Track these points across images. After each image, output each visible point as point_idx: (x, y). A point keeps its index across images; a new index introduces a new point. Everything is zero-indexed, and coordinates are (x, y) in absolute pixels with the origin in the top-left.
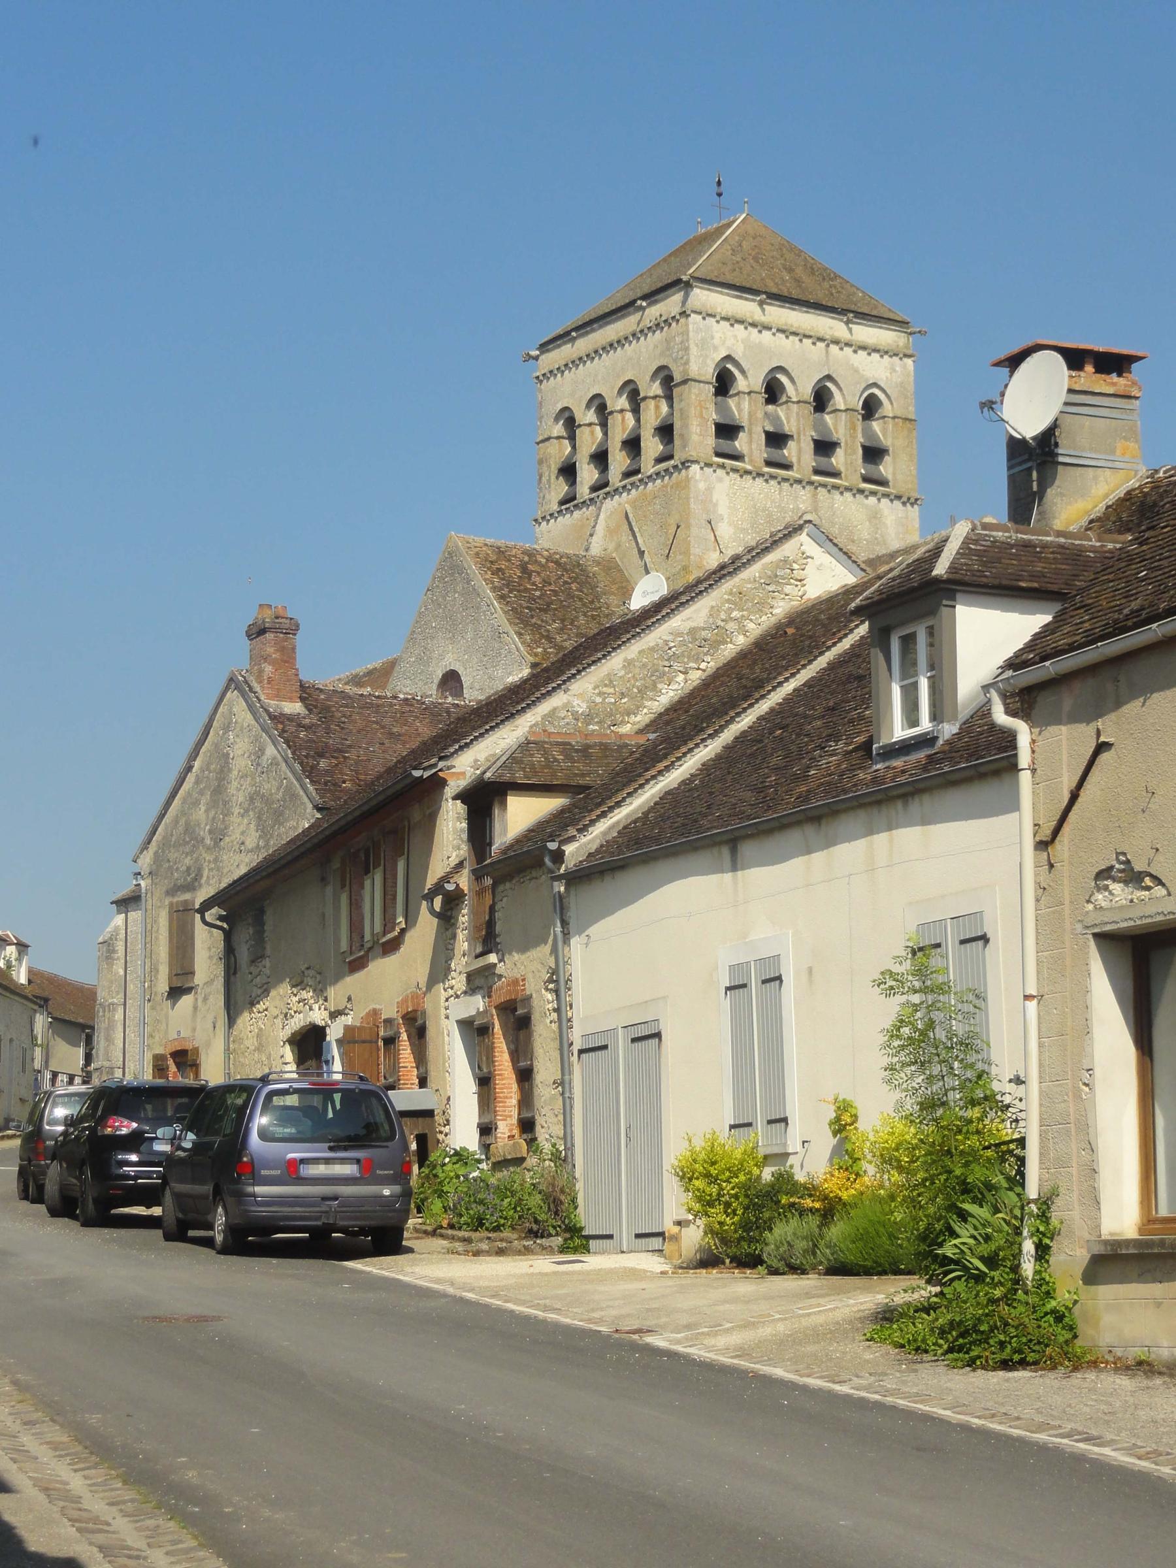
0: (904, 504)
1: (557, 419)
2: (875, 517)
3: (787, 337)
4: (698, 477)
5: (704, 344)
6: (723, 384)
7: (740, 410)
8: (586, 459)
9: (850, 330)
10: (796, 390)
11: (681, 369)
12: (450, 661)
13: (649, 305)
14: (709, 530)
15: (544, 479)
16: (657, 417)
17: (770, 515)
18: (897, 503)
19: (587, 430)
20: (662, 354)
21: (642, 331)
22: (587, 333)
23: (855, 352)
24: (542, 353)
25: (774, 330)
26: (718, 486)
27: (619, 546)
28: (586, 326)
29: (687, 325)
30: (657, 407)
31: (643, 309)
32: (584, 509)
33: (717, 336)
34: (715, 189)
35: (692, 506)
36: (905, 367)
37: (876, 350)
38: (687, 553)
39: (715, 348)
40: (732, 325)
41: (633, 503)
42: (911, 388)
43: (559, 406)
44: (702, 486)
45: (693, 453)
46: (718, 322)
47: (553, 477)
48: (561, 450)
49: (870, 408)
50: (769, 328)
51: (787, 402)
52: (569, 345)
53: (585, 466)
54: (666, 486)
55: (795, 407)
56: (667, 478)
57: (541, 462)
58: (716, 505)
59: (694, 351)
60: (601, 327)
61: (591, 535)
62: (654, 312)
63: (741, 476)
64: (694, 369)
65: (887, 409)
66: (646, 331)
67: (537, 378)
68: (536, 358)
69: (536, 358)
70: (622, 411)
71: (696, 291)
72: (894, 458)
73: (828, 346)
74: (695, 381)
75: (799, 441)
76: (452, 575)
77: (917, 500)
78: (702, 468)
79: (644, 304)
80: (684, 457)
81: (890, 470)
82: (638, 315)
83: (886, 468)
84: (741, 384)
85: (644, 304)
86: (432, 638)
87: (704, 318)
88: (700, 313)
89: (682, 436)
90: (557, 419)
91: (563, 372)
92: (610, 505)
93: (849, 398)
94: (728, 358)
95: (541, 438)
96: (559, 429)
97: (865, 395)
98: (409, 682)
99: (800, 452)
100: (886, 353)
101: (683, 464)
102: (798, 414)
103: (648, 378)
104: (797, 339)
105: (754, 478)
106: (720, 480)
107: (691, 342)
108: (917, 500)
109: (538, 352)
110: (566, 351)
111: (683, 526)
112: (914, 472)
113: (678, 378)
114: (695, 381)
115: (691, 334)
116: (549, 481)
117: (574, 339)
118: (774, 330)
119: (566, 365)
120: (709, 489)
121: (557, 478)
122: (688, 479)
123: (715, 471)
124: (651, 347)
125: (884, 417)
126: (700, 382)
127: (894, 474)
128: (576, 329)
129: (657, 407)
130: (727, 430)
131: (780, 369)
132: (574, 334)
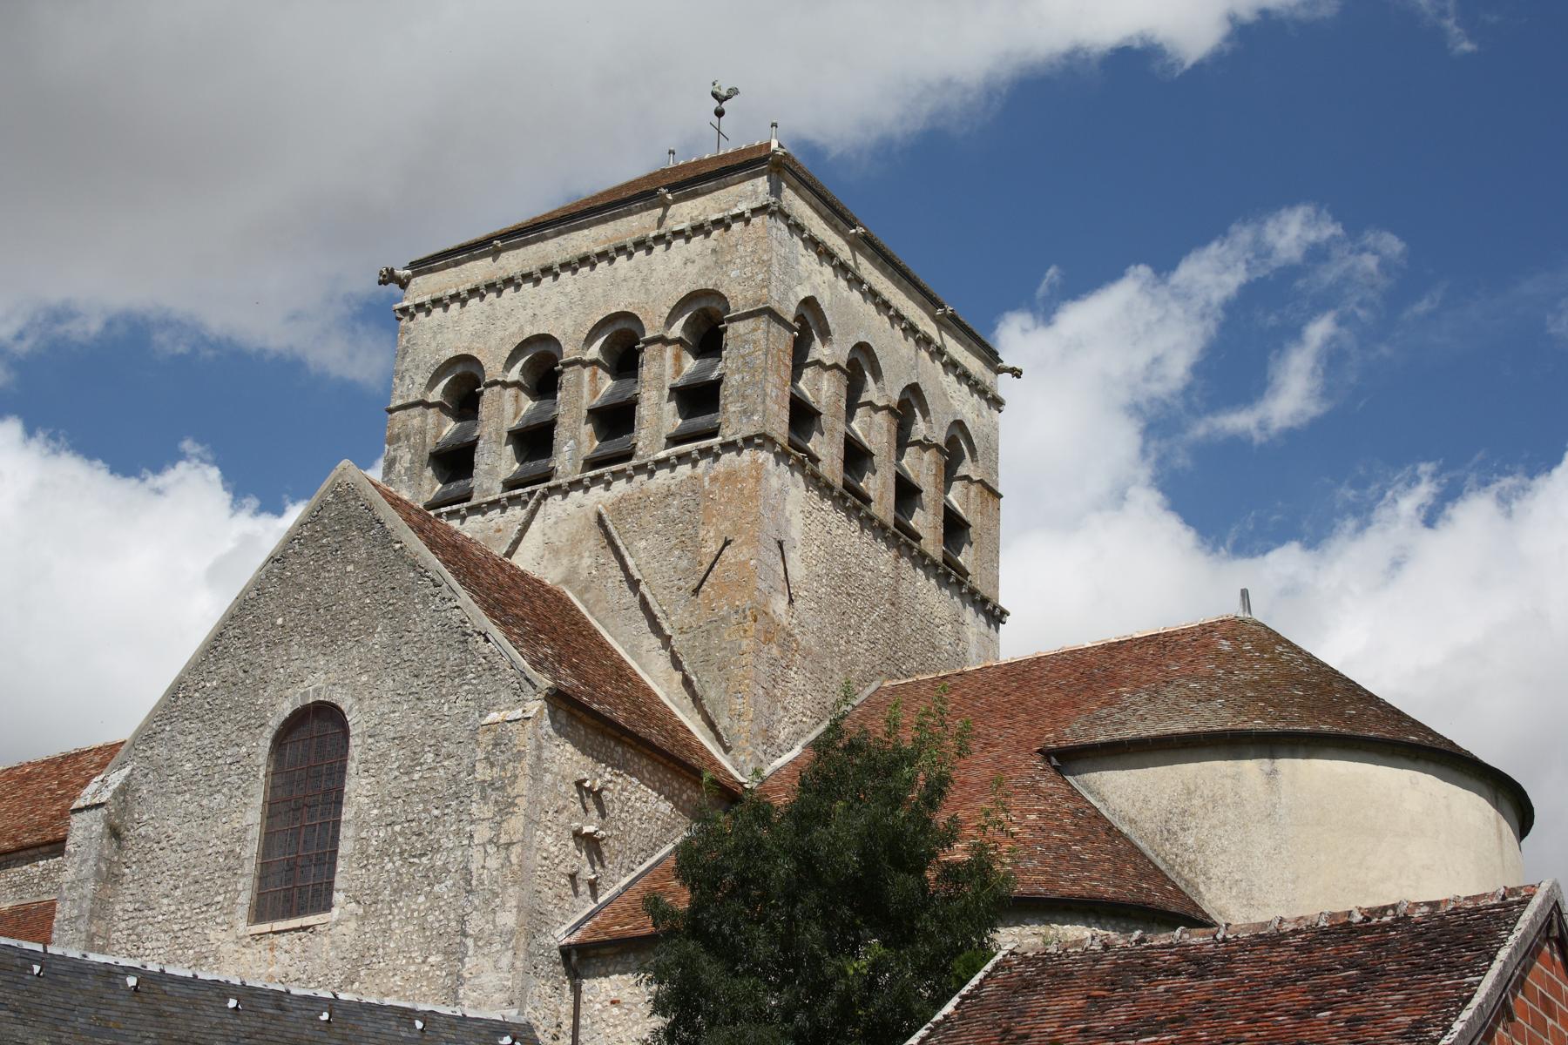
2: (957, 621)
12: (316, 686)
13: (676, 201)
17: (846, 566)
24: (416, 274)
26: (793, 491)
30: (677, 358)
31: (666, 206)
44: (775, 483)
56: (702, 464)
62: (685, 213)
67: (404, 310)
68: (403, 284)
76: (342, 532)
85: (669, 197)
94: (810, 303)
95: (399, 402)
109: (408, 272)
110: (479, 270)
113: (738, 304)
120: (783, 491)
130: (803, 415)
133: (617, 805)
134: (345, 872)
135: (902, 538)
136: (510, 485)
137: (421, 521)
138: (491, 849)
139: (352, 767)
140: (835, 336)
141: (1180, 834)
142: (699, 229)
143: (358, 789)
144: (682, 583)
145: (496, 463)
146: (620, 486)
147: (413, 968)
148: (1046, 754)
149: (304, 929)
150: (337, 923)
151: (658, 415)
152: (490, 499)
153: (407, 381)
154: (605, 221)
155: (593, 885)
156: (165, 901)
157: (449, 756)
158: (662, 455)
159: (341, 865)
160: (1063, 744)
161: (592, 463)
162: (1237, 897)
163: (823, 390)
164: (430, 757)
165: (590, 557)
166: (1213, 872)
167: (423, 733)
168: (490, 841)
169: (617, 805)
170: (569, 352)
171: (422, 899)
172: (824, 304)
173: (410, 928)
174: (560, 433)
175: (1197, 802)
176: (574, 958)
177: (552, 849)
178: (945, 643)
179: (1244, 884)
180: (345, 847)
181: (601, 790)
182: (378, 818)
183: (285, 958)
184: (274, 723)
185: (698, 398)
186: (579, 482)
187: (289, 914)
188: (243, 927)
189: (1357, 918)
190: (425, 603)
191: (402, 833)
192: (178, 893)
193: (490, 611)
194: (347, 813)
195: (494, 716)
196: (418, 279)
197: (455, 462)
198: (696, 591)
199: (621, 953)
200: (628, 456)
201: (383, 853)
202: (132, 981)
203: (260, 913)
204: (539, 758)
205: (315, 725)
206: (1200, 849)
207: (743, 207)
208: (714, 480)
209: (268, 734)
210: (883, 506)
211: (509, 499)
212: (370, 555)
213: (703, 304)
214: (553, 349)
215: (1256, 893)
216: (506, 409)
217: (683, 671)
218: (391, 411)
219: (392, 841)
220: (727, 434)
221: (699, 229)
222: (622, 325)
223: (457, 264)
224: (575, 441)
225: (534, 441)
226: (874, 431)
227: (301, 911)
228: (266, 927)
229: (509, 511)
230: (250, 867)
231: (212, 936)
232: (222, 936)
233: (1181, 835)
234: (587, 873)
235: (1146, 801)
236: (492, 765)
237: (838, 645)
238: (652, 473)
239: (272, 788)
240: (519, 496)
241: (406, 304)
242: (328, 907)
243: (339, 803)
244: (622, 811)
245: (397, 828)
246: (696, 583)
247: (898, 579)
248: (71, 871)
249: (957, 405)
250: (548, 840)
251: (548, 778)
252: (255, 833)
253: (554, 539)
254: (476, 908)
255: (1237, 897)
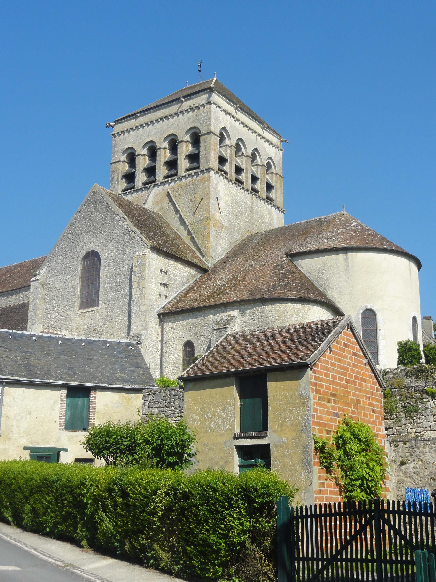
0: (279, 211)
1: (123, 153)
2: (270, 214)
3: (244, 127)
4: (213, 177)
5: (216, 118)
6: (222, 138)
7: (226, 153)
8: (141, 170)
9: (263, 132)
10: (246, 151)
11: (206, 128)
12: (92, 246)
13: (186, 101)
14: (217, 202)
15: (114, 180)
16: (187, 151)
17: (237, 202)
18: (277, 210)
19: (142, 157)
20: (193, 122)
21: (181, 112)
22: (146, 114)
23: (265, 141)
24: (116, 124)
25: (240, 122)
26: (220, 183)
27: (161, 209)
28: (143, 112)
29: (210, 108)
30: (187, 146)
31: (182, 102)
32: (140, 192)
33: (221, 117)
34: (198, 68)
35: (211, 189)
36: (279, 154)
37: (272, 144)
38: (208, 210)
39: (220, 122)
40: (226, 114)
41: (173, 189)
42: (281, 163)
43: (126, 147)
44: (215, 181)
45: (212, 166)
46: (221, 111)
47: (120, 179)
48: (124, 167)
49: (269, 166)
50: (238, 120)
51: (242, 155)
52: (134, 120)
53: (140, 173)
54: (195, 180)
55: (245, 158)
56: (195, 177)
57: (113, 172)
58: (219, 192)
59: (213, 120)
60: (154, 111)
61: (145, 204)
62: (187, 104)
63: (228, 181)
64: (213, 129)
65: (273, 170)
66: (184, 112)
67: (113, 135)
68: (113, 127)
69: (113, 127)
70: (165, 148)
71: (214, 95)
72: (275, 190)
73: (257, 136)
74: (214, 133)
75: (246, 173)
77: (284, 210)
78: (215, 173)
79: (183, 100)
80: (207, 167)
81: (274, 196)
82: (178, 106)
83: (272, 195)
84: (227, 142)
85: (183, 100)
86: (79, 235)
87: (217, 107)
88: (215, 104)
89: (205, 158)
90: (123, 153)
91: (129, 132)
92: (156, 190)
93: (263, 160)
94: (224, 128)
95: (114, 161)
96: (124, 158)
97: (267, 161)
98: (61, 257)
99: (245, 177)
100: (275, 146)
101: (207, 170)
102: (246, 161)
103: (184, 133)
104: (247, 129)
105: (232, 184)
106: (221, 181)
107: (212, 116)
108: (284, 210)
109: (114, 124)
110: (132, 123)
111: (205, 198)
112: (282, 199)
113: (203, 131)
114: (214, 133)
115: (212, 113)
116: (118, 180)
117: (138, 117)
118: (240, 122)
119: (132, 129)
120: (217, 184)
121: (122, 180)
122: (209, 177)
123: (219, 176)
124: (186, 119)
125: (273, 173)
126: (215, 134)
127: (276, 198)
128: (139, 113)
129: (187, 146)
130: (222, 160)
131: (240, 139)
132: (138, 115)
133: (172, 275)
134: (102, 296)
135: (254, 191)
136: (145, 184)
137: (117, 200)
138: (138, 289)
139: (102, 268)
140: (231, 138)
141: (322, 276)
142: (192, 109)
143: (104, 274)
144: (191, 211)
145: (141, 178)
146: (173, 184)
147: (120, 321)
148: (287, 255)
149: (92, 311)
150: (100, 309)
151: (183, 164)
152: (139, 188)
153: (116, 155)
154: (166, 107)
155: (166, 297)
156: (57, 304)
157: (126, 264)
158: (184, 174)
159: (100, 294)
160: (291, 252)
161: (166, 177)
162: (337, 292)
163: (228, 153)
164: (121, 265)
165: (167, 204)
166: (331, 286)
167: (119, 258)
168: (137, 287)
169: (172, 275)
170: (158, 146)
171: (121, 303)
172: (228, 129)
173: (119, 310)
174: (157, 169)
175: (326, 267)
176: (161, 317)
177: (154, 288)
178: (267, 221)
179: (339, 289)
180: (101, 289)
181: (167, 271)
182: (109, 281)
183: (88, 319)
184: (81, 256)
185: (194, 158)
186: (163, 183)
187: (88, 307)
188: (77, 311)
189: (306, 324)
190: (118, 223)
191: (115, 285)
192: (59, 302)
193: (136, 225)
194: (101, 280)
195: (137, 254)
196: (117, 126)
197: (130, 177)
198: (194, 213)
199: (173, 315)
200: (176, 175)
201: (111, 291)
202: (34, 338)
203: (82, 307)
204: (149, 264)
205: (92, 258)
206: (327, 280)
207: (204, 102)
208: (198, 181)
209: (80, 259)
210: (248, 184)
211: (144, 188)
212: (103, 210)
213: (194, 131)
214: (154, 145)
215: (342, 291)
216: (143, 162)
217: (192, 235)
218: (111, 164)
219: (112, 287)
220: (202, 168)
221: (192, 109)
222: (172, 137)
223: (127, 121)
224: (162, 171)
225: (151, 171)
226: (244, 163)
227: (91, 306)
228: (82, 311)
229: (144, 192)
230: (78, 295)
231: (69, 313)
232: (71, 313)
233: (322, 276)
234: (164, 293)
235: (313, 267)
236: (137, 267)
237: (235, 224)
238: (182, 179)
239: (82, 274)
240: (147, 187)
241: (114, 133)
242: (98, 305)
243: (99, 278)
244: (173, 276)
245: (114, 284)
246: (194, 210)
247: (252, 204)
248: (32, 297)
249: (269, 152)
250: (153, 286)
251: (152, 270)
252: (79, 286)
253: (157, 199)
254: (134, 305)
255: (337, 292)
